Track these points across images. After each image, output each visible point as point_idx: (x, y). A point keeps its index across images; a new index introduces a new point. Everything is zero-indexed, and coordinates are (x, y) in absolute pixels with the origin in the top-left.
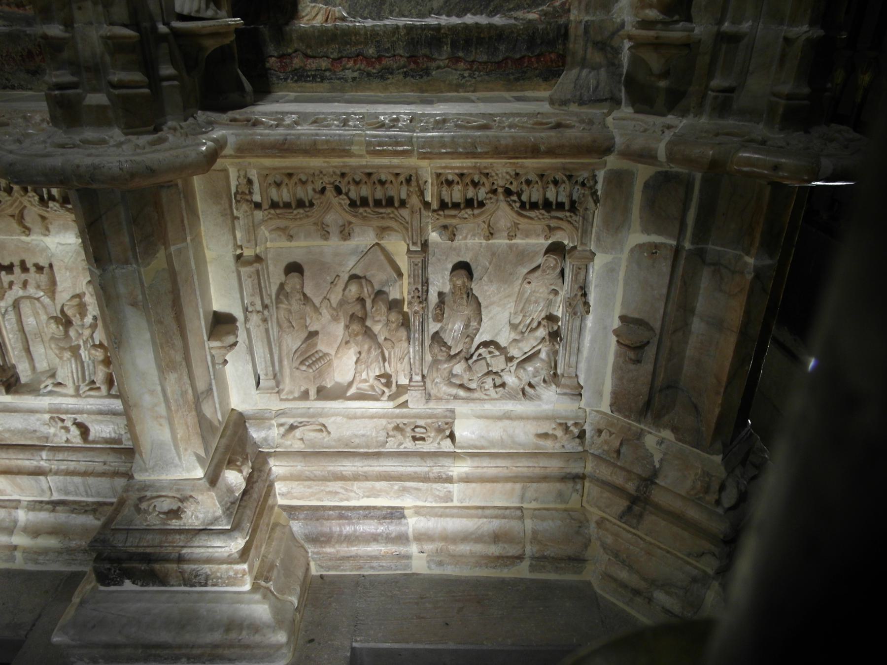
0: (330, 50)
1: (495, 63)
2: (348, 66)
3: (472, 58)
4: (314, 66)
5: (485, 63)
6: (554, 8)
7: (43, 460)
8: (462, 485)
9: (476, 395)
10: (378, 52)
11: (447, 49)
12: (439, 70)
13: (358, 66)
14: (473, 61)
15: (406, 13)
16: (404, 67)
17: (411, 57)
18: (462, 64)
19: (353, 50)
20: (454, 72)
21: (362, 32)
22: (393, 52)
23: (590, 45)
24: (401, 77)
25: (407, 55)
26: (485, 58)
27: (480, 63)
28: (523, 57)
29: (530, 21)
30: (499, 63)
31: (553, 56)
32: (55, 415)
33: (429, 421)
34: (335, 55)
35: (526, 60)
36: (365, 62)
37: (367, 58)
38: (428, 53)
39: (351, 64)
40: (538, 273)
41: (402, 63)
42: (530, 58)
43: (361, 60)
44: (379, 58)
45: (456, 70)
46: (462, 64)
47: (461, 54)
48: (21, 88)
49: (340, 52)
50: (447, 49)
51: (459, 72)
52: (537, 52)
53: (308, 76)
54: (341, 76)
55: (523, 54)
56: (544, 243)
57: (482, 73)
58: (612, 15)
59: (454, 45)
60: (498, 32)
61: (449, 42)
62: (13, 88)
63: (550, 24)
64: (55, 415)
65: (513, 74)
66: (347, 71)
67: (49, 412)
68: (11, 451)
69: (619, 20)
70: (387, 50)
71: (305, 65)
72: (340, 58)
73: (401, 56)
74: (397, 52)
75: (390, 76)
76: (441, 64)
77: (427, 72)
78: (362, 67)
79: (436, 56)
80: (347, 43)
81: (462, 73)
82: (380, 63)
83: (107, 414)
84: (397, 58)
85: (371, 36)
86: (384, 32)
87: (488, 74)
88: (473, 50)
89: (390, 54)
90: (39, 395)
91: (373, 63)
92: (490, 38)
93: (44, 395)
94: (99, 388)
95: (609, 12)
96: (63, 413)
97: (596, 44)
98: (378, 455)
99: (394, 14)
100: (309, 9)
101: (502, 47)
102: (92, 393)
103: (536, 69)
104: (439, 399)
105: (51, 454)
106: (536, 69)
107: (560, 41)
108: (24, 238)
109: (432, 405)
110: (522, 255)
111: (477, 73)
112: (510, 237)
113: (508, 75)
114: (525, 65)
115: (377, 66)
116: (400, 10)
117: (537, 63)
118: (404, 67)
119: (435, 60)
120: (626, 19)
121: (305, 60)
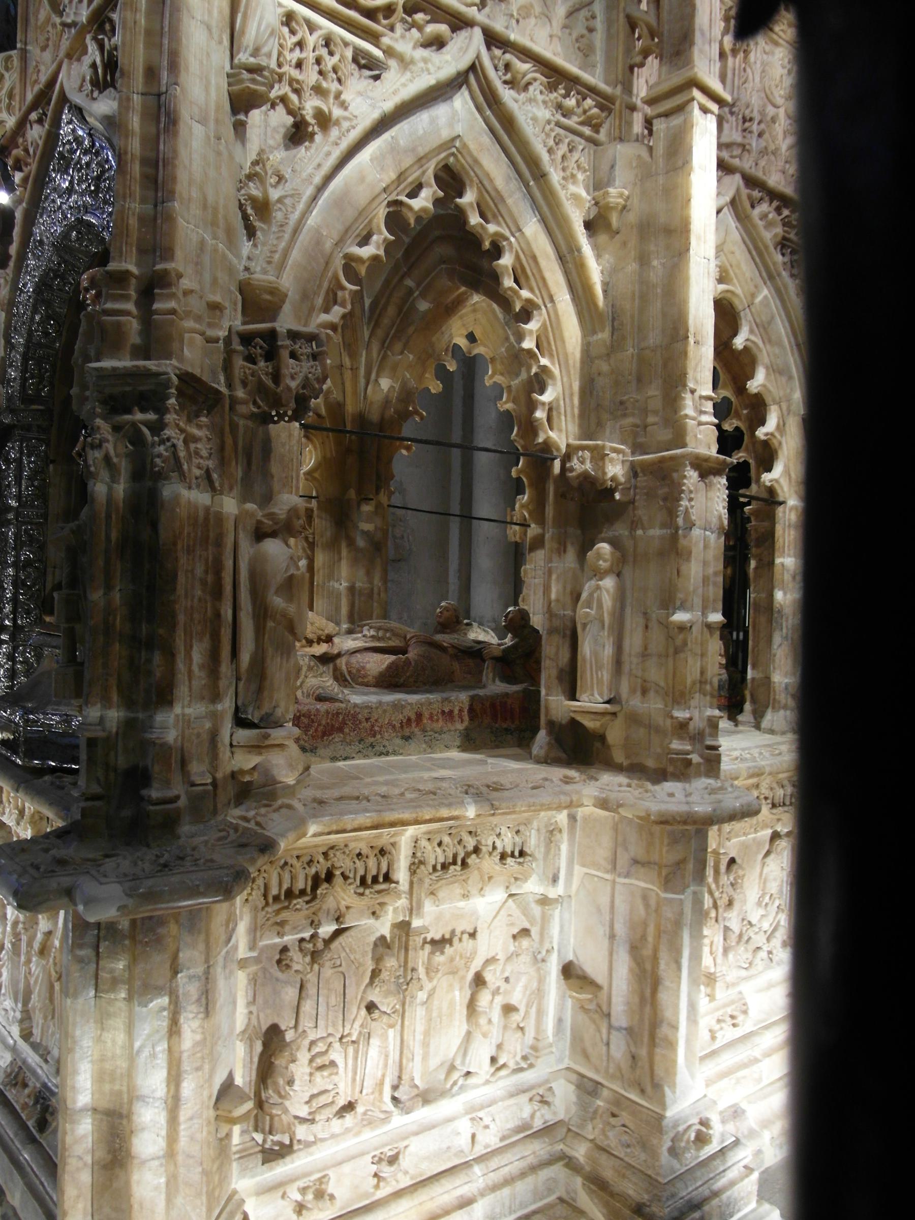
7: (478, 1178)
8: (767, 1059)
9: (752, 971)
32: (474, 1115)
33: (733, 1007)
40: (772, 856)
48: (395, 753)
56: (769, 832)
62: (387, 754)
64: (474, 1115)
67: (467, 1113)
68: (443, 1181)
83: (517, 1094)
90: (453, 1096)
93: (458, 1094)
94: (504, 1066)
96: (480, 1110)
98: (713, 1054)
102: (503, 1073)
104: (734, 985)
105: (482, 1165)
108: (462, 904)
109: (730, 991)
110: (758, 843)
112: (756, 831)
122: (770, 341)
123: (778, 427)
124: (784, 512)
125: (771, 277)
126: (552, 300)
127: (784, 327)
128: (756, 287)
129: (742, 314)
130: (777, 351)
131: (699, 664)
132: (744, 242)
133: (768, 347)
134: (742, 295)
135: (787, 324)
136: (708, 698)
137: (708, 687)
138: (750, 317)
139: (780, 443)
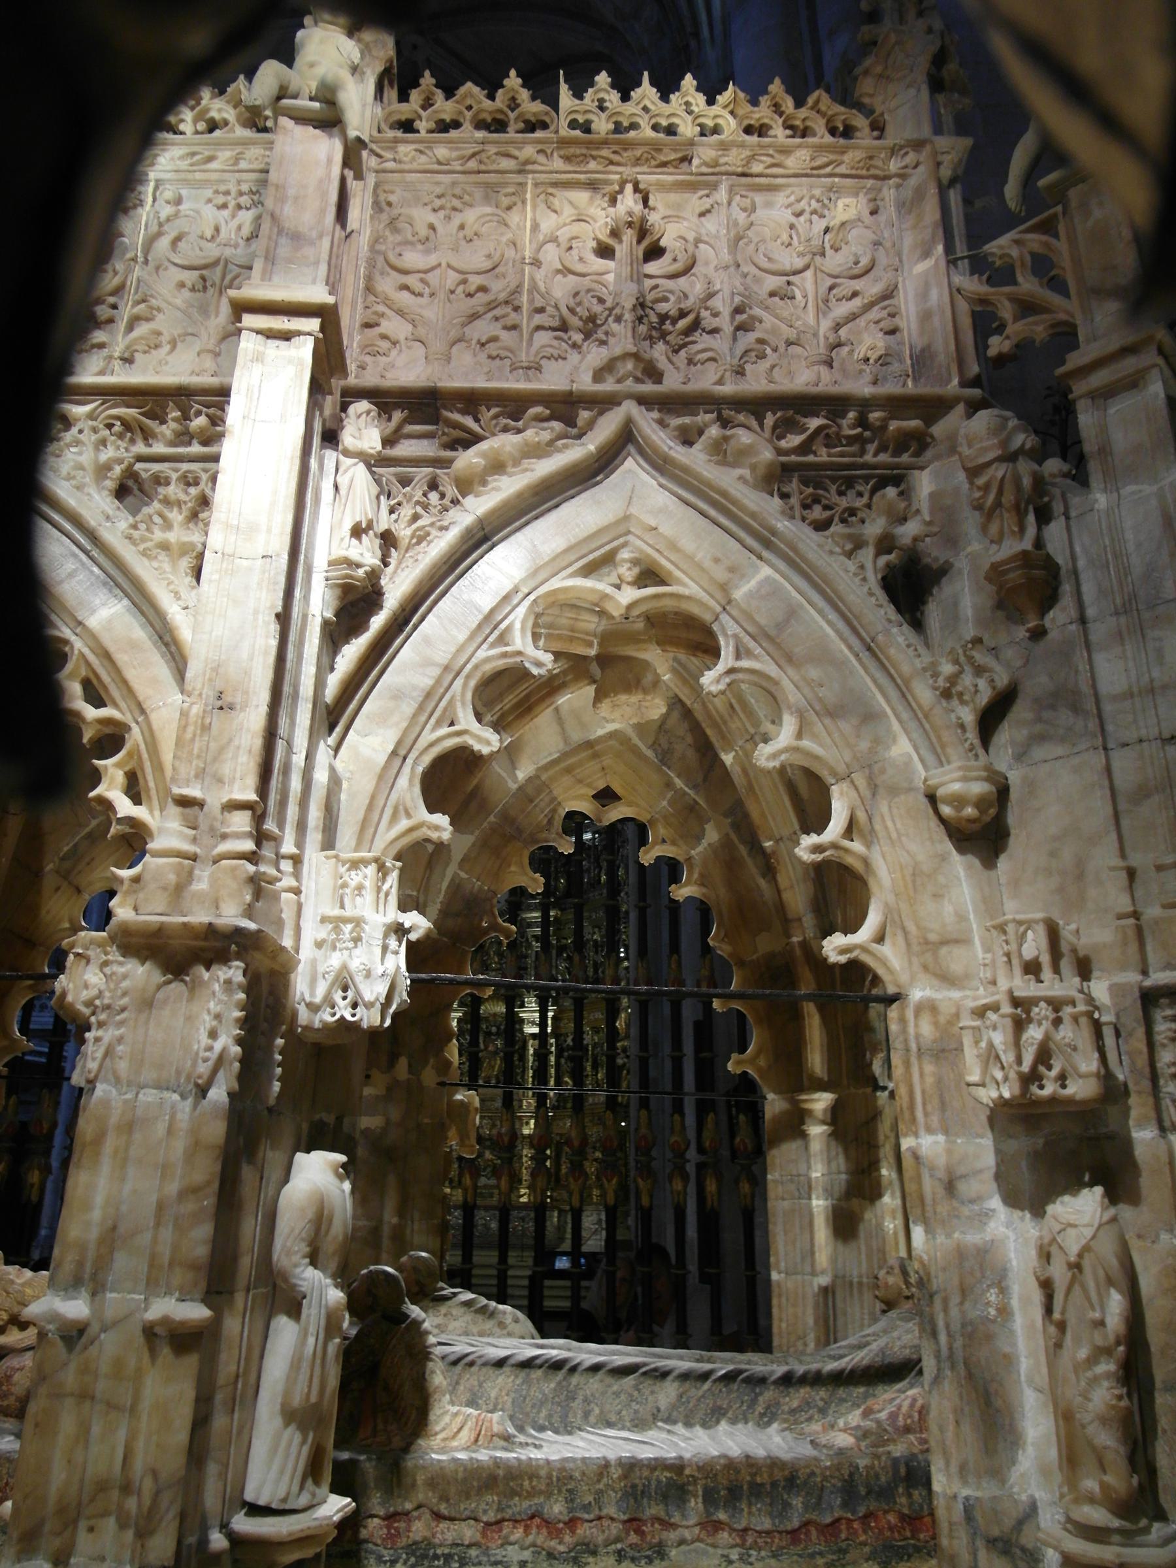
0: (483, 1506)
1: (788, 1532)
2: (512, 1538)
3: (743, 1524)
4: (450, 1537)
5: (768, 1533)
6: (878, 1422)
10: (570, 1510)
11: (695, 1505)
12: (683, 1548)
13: (531, 1538)
14: (745, 1530)
15: (613, 1418)
16: (618, 1540)
17: (630, 1520)
18: (726, 1535)
19: (520, 1506)
20: (711, 1550)
21: (543, 1473)
22: (597, 1512)
23: (980, 1543)
24: (611, 1560)
25: (625, 1517)
26: (766, 1524)
27: (759, 1532)
28: (838, 1520)
29: (841, 1452)
30: (793, 1535)
31: (892, 1518)
34: (491, 1516)
35: (843, 1527)
36: (544, 1531)
37: (548, 1524)
38: (662, 1514)
39: (518, 1533)
41: (614, 1532)
42: (849, 1521)
43: (538, 1527)
44: (572, 1523)
45: (714, 1546)
46: (726, 1535)
47: (722, 1516)
49: (500, 1509)
50: (695, 1505)
51: (720, 1551)
52: (862, 1511)
53: (436, 1557)
54: (499, 1558)
55: (836, 1515)
57: (763, 1553)
58: (1012, 1487)
59: (710, 1498)
60: (786, 1473)
61: (700, 1493)
63: (877, 1456)
65: (821, 1554)
66: (510, 1548)
69: (1024, 1497)
70: (586, 1508)
71: (434, 1536)
72: (498, 1522)
73: (612, 1519)
74: (604, 1512)
75: (591, 1560)
76: (687, 1534)
77: (660, 1551)
78: (540, 1540)
79: (676, 1518)
80: (514, 1493)
81: (726, 1552)
82: (573, 1532)
84: (605, 1523)
85: (558, 1479)
86: (584, 1474)
87: (775, 1555)
88: (744, 1506)
89: (592, 1516)
91: (560, 1531)
92: (774, 1484)
95: (1004, 1482)
97: (992, 1542)
99: (592, 1419)
100: (447, 1419)
101: (797, 1502)
103: (864, 1544)
106: (864, 1544)
107: (901, 1490)
111: (753, 1552)
113: (812, 1556)
114: (843, 1536)
115: (568, 1539)
116: (602, 1412)
117: (865, 1532)
118: (618, 1540)
119: (674, 1526)
120: (1037, 1496)
121: (434, 1524)
122: (790, 658)
123: (850, 831)
124: (903, 1020)
125: (768, 544)
126: (143, 711)
127: (829, 623)
128: (732, 570)
129: (715, 627)
130: (814, 673)
131: (121, 1435)
132: (687, 503)
133: (791, 671)
134: (702, 595)
135: (833, 616)
136: (129, 1535)
137: (131, 1504)
138: (732, 627)
139: (866, 862)
